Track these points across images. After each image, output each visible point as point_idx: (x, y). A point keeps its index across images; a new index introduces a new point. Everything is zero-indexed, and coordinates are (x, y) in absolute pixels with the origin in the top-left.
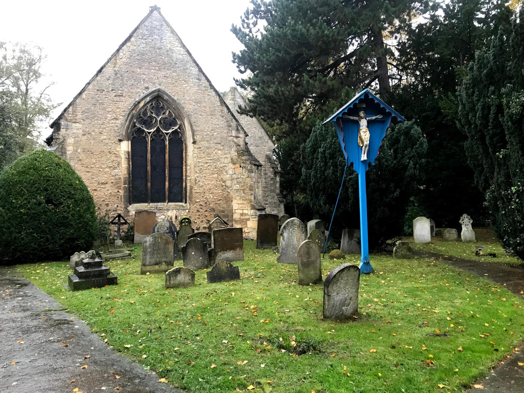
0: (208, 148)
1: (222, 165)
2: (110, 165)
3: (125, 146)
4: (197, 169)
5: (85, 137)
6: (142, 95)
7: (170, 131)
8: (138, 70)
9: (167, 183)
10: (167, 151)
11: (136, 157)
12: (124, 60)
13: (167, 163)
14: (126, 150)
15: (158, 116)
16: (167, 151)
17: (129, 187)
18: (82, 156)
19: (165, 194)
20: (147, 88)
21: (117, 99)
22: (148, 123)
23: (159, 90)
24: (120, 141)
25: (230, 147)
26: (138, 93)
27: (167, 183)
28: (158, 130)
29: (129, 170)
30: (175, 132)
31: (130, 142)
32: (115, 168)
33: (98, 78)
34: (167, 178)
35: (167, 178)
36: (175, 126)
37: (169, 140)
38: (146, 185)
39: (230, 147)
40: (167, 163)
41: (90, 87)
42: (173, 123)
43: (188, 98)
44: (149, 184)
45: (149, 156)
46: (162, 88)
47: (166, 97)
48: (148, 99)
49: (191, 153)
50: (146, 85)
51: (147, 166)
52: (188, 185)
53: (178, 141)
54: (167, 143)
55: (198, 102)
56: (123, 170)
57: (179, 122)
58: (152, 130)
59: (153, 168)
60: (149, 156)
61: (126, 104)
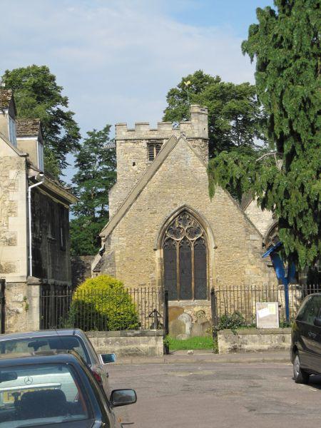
0: (227, 252)
1: (240, 266)
2: (148, 269)
3: (159, 254)
4: (218, 271)
5: (128, 249)
6: (173, 211)
7: (195, 239)
8: (169, 190)
9: (193, 284)
10: (193, 256)
11: (167, 262)
12: (157, 183)
13: (193, 266)
14: (159, 257)
15: (185, 226)
16: (193, 256)
17: (162, 288)
18: (127, 263)
19: (191, 292)
20: (175, 205)
21: (151, 216)
22: (176, 233)
23: (185, 206)
24: (155, 250)
25: (248, 249)
26: (168, 210)
27: (193, 284)
28: (185, 238)
29: (161, 273)
30: (200, 239)
31: (162, 250)
32: (151, 272)
33: (137, 200)
34: (193, 279)
35: (193, 279)
36: (199, 234)
37: (194, 247)
38: (176, 285)
39: (248, 249)
40: (193, 266)
41: (132, 208)
42: (197, 232)
43: (209, 209)
44: (178, 285)
45: (178, 261)
46: (188, 203)
47: (191, 211)
48: (176, 214)
49: (213, 255)
50: (174, 202)
51: (176, 269)
52: (211, 284)
53: (202, 247)
54: (192, 249)
55: (218, 212)
56: (157, 273)
57: (202, 230)
58: (180, 239)
59: (182, 271)
60: (178, 261)
61: (159, 220)
